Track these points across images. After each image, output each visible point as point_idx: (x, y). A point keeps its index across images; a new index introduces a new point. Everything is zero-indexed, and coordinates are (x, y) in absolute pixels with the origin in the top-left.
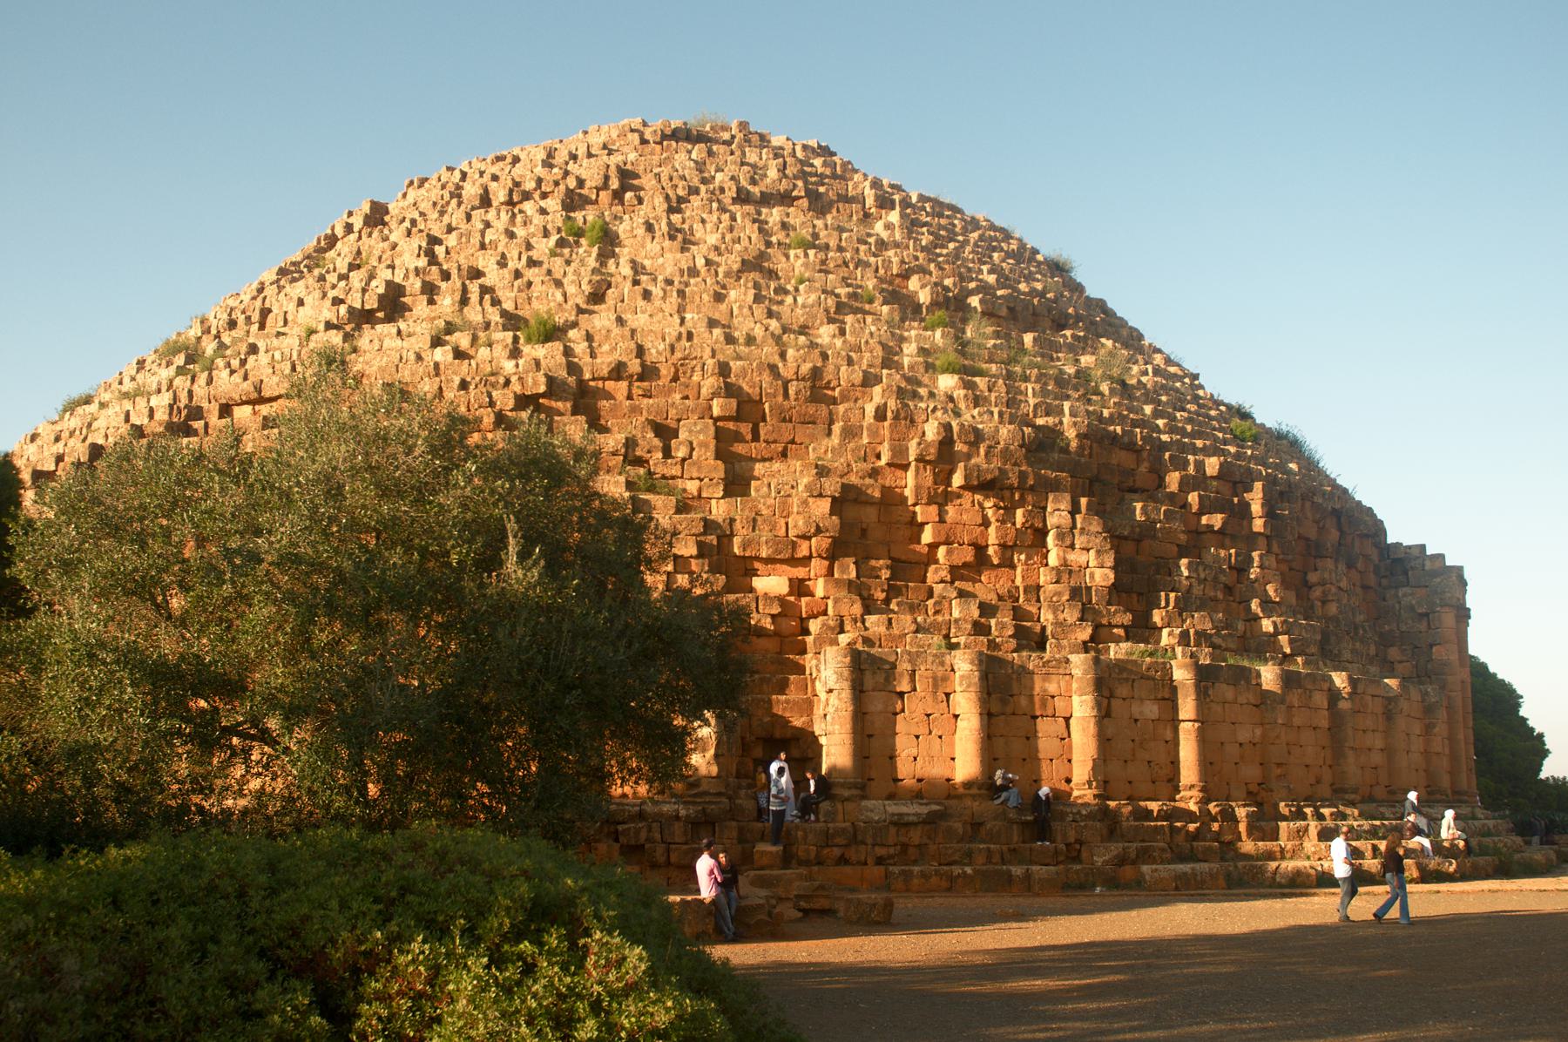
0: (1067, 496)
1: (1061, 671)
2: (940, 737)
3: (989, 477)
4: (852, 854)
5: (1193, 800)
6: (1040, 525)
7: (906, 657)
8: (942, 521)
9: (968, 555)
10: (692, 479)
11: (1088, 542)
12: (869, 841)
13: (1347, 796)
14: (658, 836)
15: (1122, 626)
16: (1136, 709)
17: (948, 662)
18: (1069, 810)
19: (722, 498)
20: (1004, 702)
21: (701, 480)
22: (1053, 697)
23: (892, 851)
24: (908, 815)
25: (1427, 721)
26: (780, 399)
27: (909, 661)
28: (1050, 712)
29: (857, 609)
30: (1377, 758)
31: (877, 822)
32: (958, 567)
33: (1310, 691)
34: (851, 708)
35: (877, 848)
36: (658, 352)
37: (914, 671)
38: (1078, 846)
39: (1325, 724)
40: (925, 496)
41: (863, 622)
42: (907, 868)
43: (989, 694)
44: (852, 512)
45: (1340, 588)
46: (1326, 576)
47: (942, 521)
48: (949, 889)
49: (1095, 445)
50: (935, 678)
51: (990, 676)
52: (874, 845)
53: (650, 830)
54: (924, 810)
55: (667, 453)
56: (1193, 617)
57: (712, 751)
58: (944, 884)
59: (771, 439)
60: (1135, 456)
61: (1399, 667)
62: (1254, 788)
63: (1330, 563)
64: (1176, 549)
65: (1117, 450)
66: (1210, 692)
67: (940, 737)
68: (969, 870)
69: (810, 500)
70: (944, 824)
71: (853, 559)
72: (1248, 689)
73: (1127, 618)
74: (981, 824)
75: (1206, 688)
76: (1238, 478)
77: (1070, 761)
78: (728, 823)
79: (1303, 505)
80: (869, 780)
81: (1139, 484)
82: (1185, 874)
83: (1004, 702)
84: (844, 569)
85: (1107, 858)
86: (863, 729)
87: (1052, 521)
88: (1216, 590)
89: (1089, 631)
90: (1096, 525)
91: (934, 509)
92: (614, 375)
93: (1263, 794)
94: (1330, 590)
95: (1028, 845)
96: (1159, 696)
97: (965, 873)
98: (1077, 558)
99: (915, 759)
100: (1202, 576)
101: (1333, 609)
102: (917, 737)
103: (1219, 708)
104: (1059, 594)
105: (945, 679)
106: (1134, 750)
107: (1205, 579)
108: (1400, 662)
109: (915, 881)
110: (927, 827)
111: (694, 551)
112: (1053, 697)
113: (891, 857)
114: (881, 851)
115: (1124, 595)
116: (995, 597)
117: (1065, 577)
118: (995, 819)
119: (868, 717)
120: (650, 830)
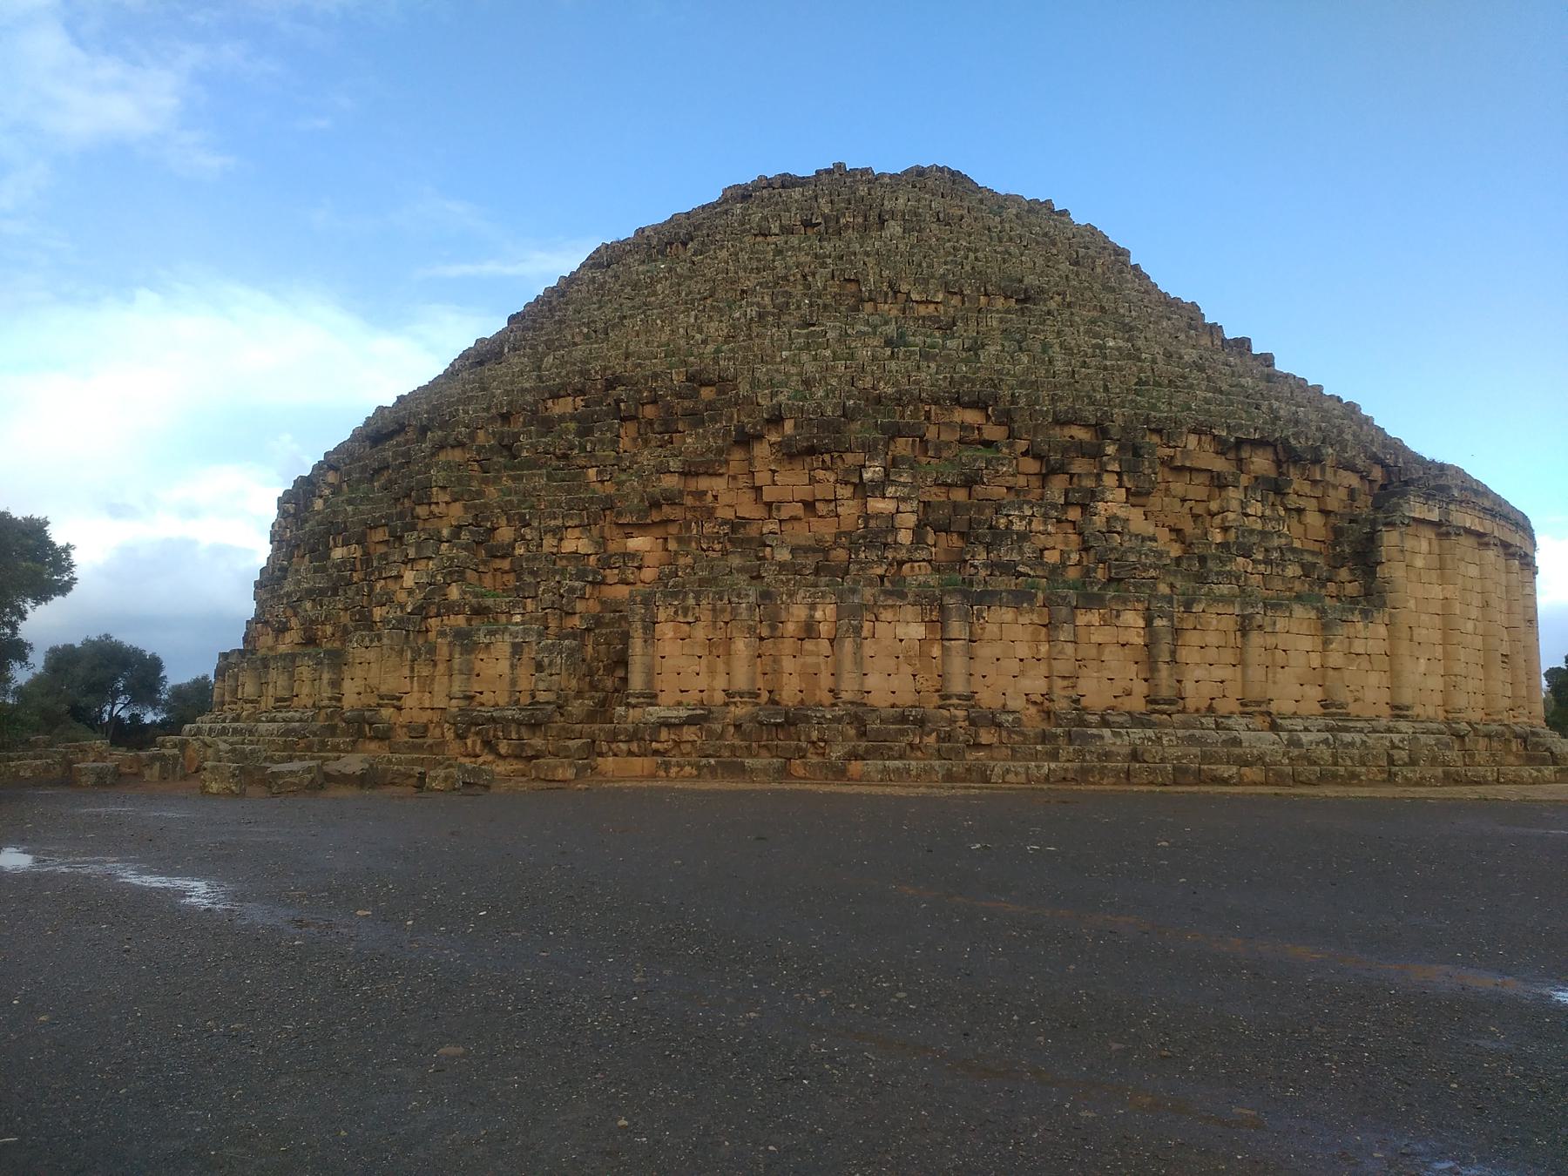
1: (828, 601)
6: (856, 480)
7: (691, 595)
8: (774, 483)
9: (798, 510)
11: (896, 492)
12: (647, 738)
13: (1157, 707)
15: (924, 560)
16: (901, 631)
18: (813, 715)
21: (596, 466)
22: (820, 622)
23: (665, 745)
27: (694, 598)
28: (813, 635)
31: (653, 723)
33: (1118, 611)
35: (654, 743)
37: (699, 605)
38: (822, 744)
41: (693, 568)
43: (761, 622)
45: (1247, 515)
46: (1224, 504)
48: (698, 776)
51: (762, 607)
52: (651, 741)
53: (495, 730)
58: (695, 772)
65: (960, 409)
68: (712, 761)
70: (706, 725)
72: (1032, 611)
74: (740, 725)
75: (980, 612)
78: (552, 725)
79: (1200, 440)
80: (662, 691)
81: (986, 436)
82: (898, 769)
83: (773, 627)
87: (867, 475)
88: (1045, 523)
93: (1047, 703)
96: (926, 620)
98: (885, 506)
99: (698, 674)
103: (995, 628)
104: (864, 537)
107: (1033, 515)
112: (820, 622)
113: (667, 751)
118: (750, 722)
120: (495, 730)
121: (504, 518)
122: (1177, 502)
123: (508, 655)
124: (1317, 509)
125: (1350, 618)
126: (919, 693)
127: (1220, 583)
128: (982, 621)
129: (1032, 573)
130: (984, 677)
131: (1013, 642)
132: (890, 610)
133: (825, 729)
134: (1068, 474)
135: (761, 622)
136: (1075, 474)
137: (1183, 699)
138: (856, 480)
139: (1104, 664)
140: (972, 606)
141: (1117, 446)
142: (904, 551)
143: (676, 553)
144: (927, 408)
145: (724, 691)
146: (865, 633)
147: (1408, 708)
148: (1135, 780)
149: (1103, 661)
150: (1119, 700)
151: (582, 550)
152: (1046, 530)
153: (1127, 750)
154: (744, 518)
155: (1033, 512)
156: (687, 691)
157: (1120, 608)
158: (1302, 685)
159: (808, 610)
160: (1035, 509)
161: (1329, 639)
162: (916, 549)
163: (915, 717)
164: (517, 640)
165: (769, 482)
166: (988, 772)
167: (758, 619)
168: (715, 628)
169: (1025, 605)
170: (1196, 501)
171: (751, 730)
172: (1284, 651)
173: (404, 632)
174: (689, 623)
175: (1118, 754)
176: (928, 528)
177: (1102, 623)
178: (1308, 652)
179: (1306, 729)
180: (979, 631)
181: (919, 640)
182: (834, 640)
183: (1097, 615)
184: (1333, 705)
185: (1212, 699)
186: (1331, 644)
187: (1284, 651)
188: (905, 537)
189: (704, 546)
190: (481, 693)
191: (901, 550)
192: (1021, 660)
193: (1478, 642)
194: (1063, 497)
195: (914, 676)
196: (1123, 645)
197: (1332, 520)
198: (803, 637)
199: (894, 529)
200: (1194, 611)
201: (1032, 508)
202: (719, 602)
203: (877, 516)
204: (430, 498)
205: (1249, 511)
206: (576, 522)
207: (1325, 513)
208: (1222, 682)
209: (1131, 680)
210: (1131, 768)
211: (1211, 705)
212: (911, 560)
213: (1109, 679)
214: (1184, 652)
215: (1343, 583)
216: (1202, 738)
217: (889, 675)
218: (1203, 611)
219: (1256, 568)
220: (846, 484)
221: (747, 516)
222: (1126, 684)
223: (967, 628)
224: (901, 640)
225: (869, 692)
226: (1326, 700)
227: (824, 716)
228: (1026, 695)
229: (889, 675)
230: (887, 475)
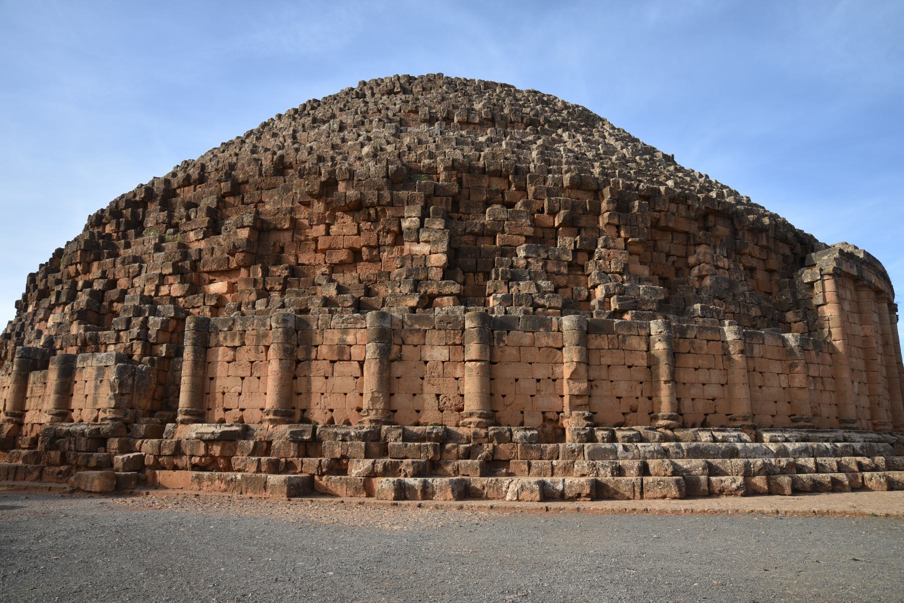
0: (419, 207)
1: (359, 326)
2: (259, 378)
3: (354, 199)
4: (176, 461)
5: (472, 426)
6: (396, 229)
8: (328, 233)
10: (192, 230)
11: (429, 236)
12: (188, 453)
14: (73, 446)
15: (451, 294)
17: (268, 323)
19: (202, 239)
20: (309, 352)
22: (351, 346)
24: (207, 433)
25: (789, 362)
26: (257, 177)
27: (241, 324)
29: (253, 297)
30: (713, 391)
32: (334, 264)
33: (624, 336)
34: (192, 357)
36: (212, 167)
37: (245, 331)
39: (644, 363)
40: (315, 219)
41: (254, 304)
42: (201, 473)
44: (274, 237)
45: (717, 267)
46: (701, 257)
47: (328, 233)
49: (464, 175)
50: (258, 336)
51: (300, 332)
52: (192, 456)
54: (219, 430)
55: (188, 218)
56: (519, 285)
57: (117, 392)
58: (223, 486)
59: (249, 201)
60: (506, 181)
61: (795, 326)
62: (551, 416)
63: (702, 249)
64: (524, 239)
67: (259, 378)
69: (238, 230)
71: (260, 265)
72: (548, 336)
73: (455, 288)
76: (595, 187)
77: (361, 395)
80: (209, 409)
84: (255, 273)
85: (360, 471)
86: (205, 373)
87: (405, 224)
88: (559, 266)
89: (417, 299)
90: (438, 224)
91: (322, 227)
92: (186, 183)
94: (703, 267)
95: (300, 459)
97: (236, 478)
98: (421, 249)
99: (240, 394)
100: (544, 256)
101: (708, 282)
102: (243, 378)
103: (514, 351)
105: (265, 336)
106: (421, 385)
107: (548, 258)
108: (795, 322)
109: (205, 483)
110: (228, 444)
111: (170, 270)
112: (351, 346)
114: (196, 460)
115: (471, 275)
116: (356, 281)
117: (408, 263)
119: (210, 365)
120: (70, 443)
121: (123, 271)
122: (663, 256)
123: (94, 377)
126: (442, 411)
127: (705, 317)
128: (502, 344)
129: (547, 304)
130: (504, 396)
131: (530, 363)
132: (416, 334)
133: (349, 446)
134: (576, 227)
135: (298, 346)
136: (582, 227)
137: (682, 415)
138: (396, 229)
139: (613, 383)
140: (492, 331)
141: (615, 205)
142: (435, 286)
143: (242, 291)
144: (460, 175)
145: (262, 409)
146: (393, 356)
147: (854, 422)
148: (650, 494)
149: (612, 381)
150: (628, 417)
151: (174, 294)
153: (637, 463)
154: (303, 265)
155: (548, 256)
156: (230, 409)
157: (625, 333)
159: (340, 335)
160: (550, 253)
161: (795, 363)
162: (445, 285)
163: (437, 434)
164: (100, 365)
165: (324, 233)
166: (504, 489)
167: (295, 343)
168: (257, 350)
169: (541, 330)
170: (678, 257)
171: (280, 446)
172: (760, 373)
173: (31, 361)
174: (234, 348)
175: (632, 468)
176: (458, 269)
177: (610, 347)
179: (787, 440)
180: (500, 353)
181: (443, 362)
182: (363, 361)
183: (606, 339)
184: (801, 419)
185: (706, 415)
186: (797, 366)
187: (760, 373)
188: (436, 274)
189: (268, 287)
190: (73, 410)
191: (432, 285)
192: (538, 380)
193: (884, 370)
194: (573, 245)
195: (438, 396)
196: (629, 367)
197: (776, 277)
198: (336, 358)
199: (426, 268)
200: (688, 337)
201: (547, 252)
202: (262, 328)
203: (412, 257)
204: (76, 260)
205: (720, 264)
206: (170, 270)
207: (771, 271)
208: (713, 400)
209: (637, 398)
210: (645, 482)
211: (705, 420)
212: (441, 295)
213: (617, 398)
214: (682, 374)
215: (790, 323)
217: (414, 395)
218: (695, 338)
219: (728, 308)
220: (388, 233)
221: (307, 263)
222: (633, 402)
223: (488, 350)
224: (426, 362)
225: (396, 411)
226: (795, 415)
227: (348, 434)
228: (543, 413)
229: (414, 395)
230: (422, 225)
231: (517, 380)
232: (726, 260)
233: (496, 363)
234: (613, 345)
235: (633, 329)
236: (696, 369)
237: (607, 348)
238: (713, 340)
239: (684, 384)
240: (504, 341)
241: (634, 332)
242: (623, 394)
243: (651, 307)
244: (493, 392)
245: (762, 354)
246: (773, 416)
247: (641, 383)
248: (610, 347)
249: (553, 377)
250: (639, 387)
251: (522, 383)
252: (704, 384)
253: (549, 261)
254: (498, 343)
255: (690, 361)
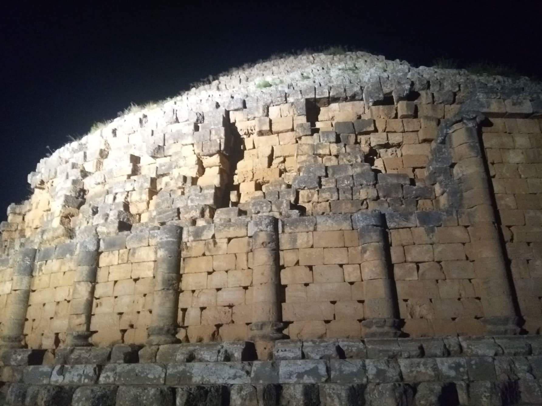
66: (43, 268)
107: (134, 190)
124: (417, 141)
125: (404, 224)
128: (41, 273)
149: (116, 297)
152: (141, 199)
157: (135, 246)
158: (334, 303)
178: (341, 266)
192: (58, 303)
196: (136, 280)
200: (203, 238)
208: (231, 306)
209: (139, 312)
216: (142, 373)
231: (44, 305)
232: (335, 145)
233: (34, 291)
234: (122, 260)
235: (144, 241)
236: (210, 273)
237: (116, 263)
238: (236, 237)
239: (193, 291)
240: (42, 270)
241: (145, 243)
242: (124, 310)
243: (194, 214)
244: (28, 317)
245: (311, 243)
246: (327, 322)
247: (145, 295)
248: (120, 262)
249: (68, 299)
250: (142, 300)
251: (47, 307)
252: (218, 290)
253: (134, 192)
254: (39, 273)
255: (204, 265)
